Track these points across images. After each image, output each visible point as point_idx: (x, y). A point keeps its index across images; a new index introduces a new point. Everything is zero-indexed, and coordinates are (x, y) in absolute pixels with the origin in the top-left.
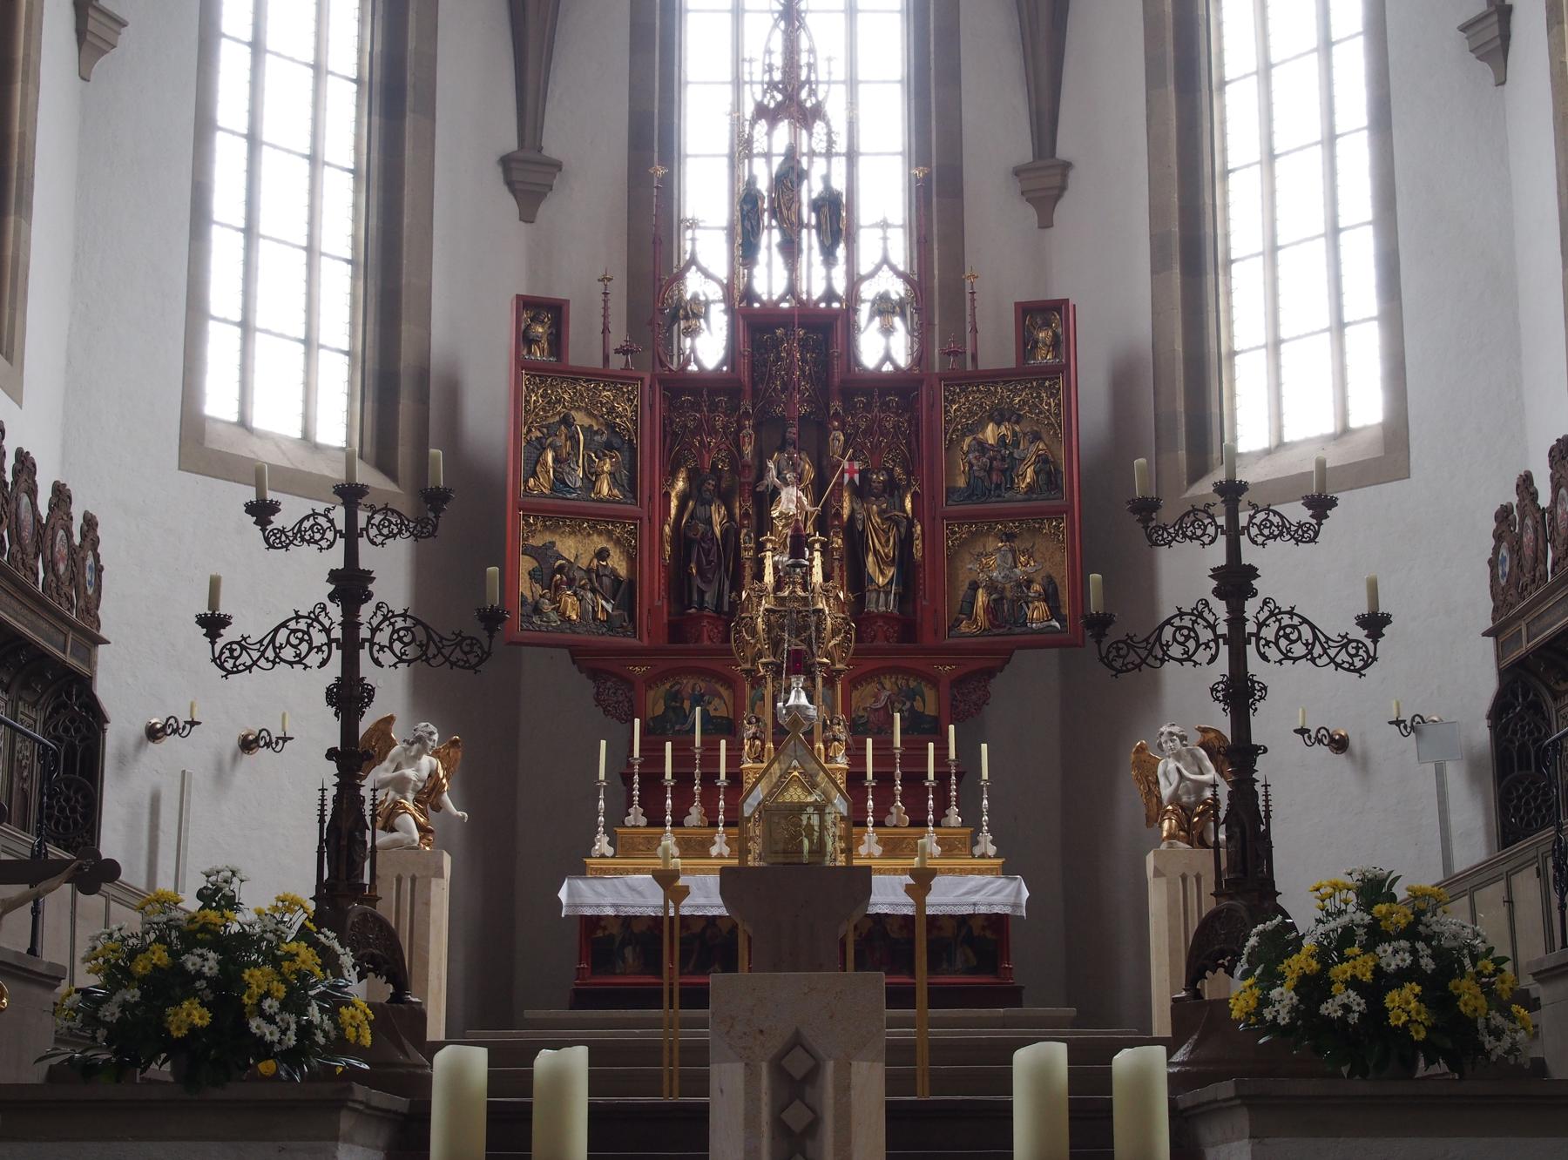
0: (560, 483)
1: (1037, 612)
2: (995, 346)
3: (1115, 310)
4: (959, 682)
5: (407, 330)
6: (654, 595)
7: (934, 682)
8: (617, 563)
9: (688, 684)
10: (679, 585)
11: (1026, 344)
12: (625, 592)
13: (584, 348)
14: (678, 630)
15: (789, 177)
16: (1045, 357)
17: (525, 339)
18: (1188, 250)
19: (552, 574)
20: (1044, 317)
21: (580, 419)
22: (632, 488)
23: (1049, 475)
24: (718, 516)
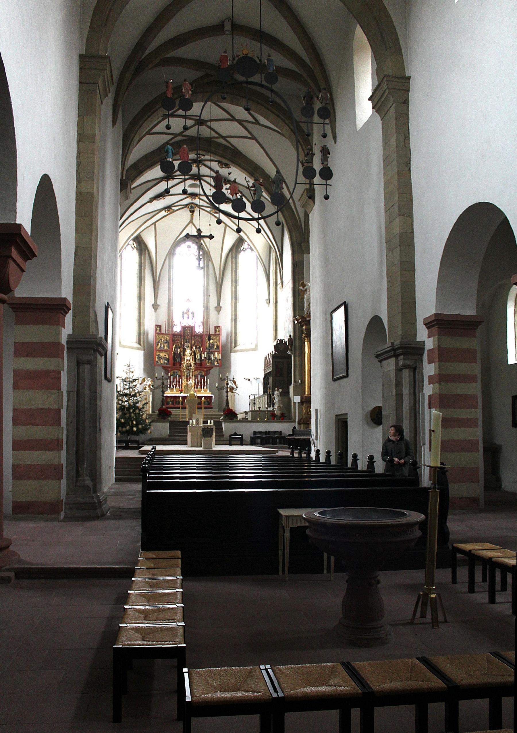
0: (160, 347)
1: (216, 363)
2: (212, 332)
3: (226, 328)
4: (207, 371)
5: (142, 328)
6: (171, 361)
7: (204, 371)
8: (167, 357)
9: (175, 371)
10: (174, 358)
11: (215, 331)
12: (168, 360)
13: (163, 331)
14: (174, 364)
15: (188, 310)
16: (218, 333)
17: (156, 330)
18: (235, 319)
19: (160, 358)
20: (217, 328)
21: (163, 339)
22: (169, 347)
23: (217, 346)
24: (179, 350)
